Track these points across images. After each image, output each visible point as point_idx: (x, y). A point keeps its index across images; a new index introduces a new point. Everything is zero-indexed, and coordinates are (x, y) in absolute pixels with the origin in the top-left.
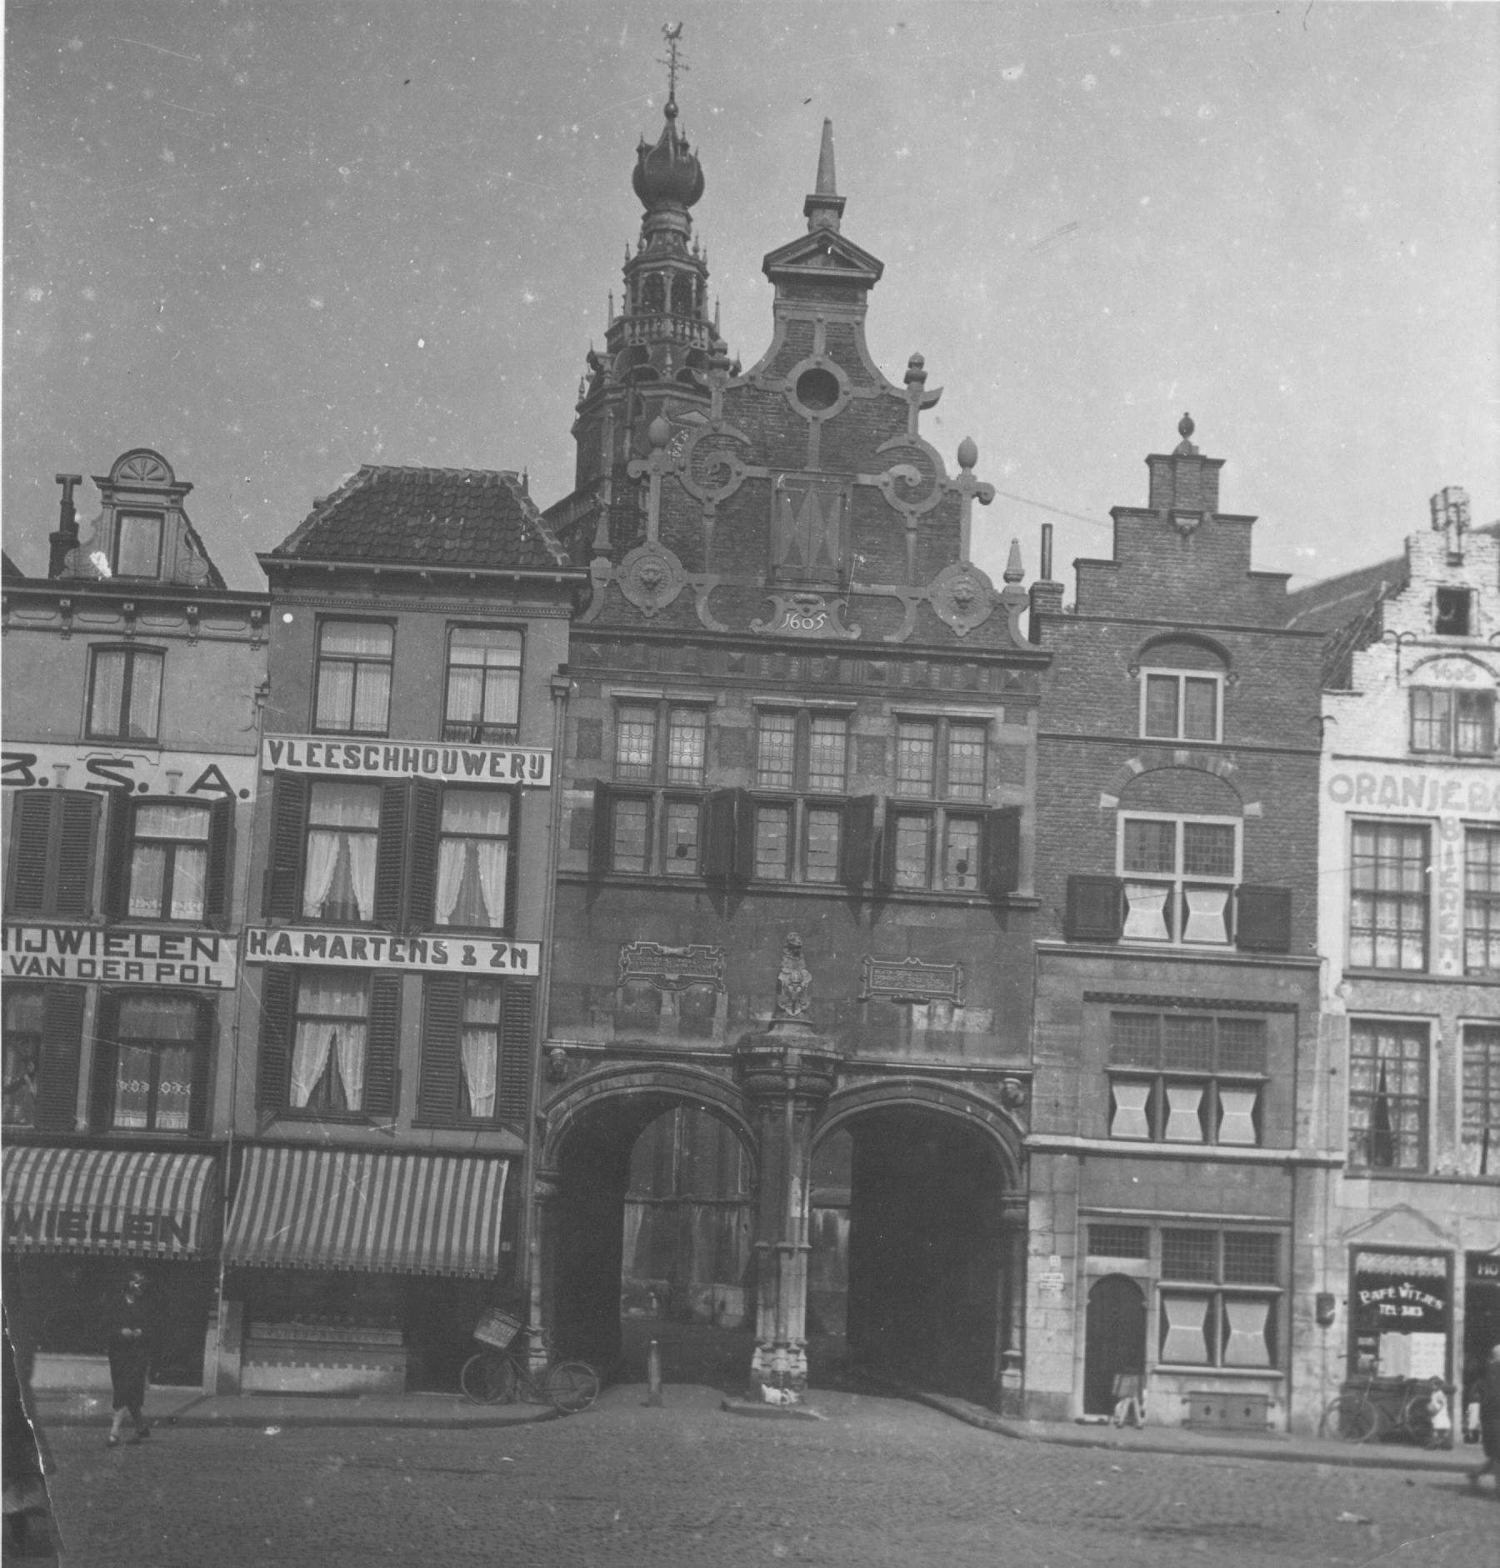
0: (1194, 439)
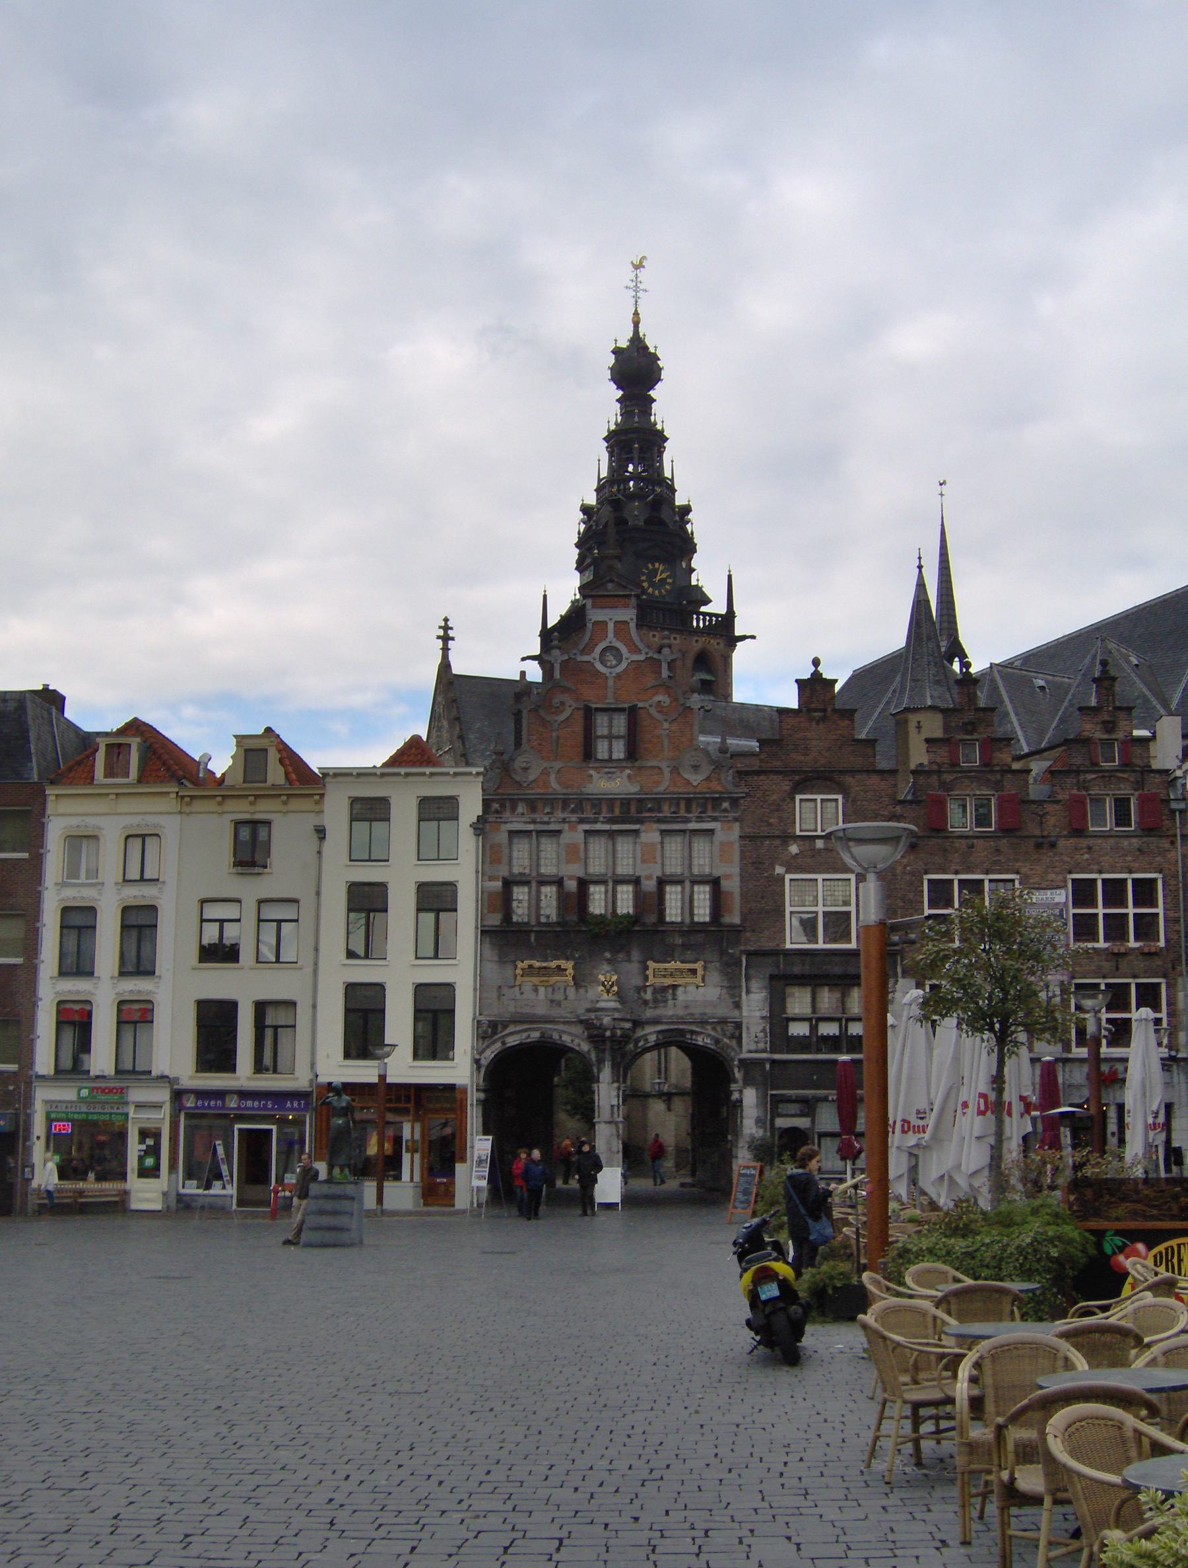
0: (819, 669)
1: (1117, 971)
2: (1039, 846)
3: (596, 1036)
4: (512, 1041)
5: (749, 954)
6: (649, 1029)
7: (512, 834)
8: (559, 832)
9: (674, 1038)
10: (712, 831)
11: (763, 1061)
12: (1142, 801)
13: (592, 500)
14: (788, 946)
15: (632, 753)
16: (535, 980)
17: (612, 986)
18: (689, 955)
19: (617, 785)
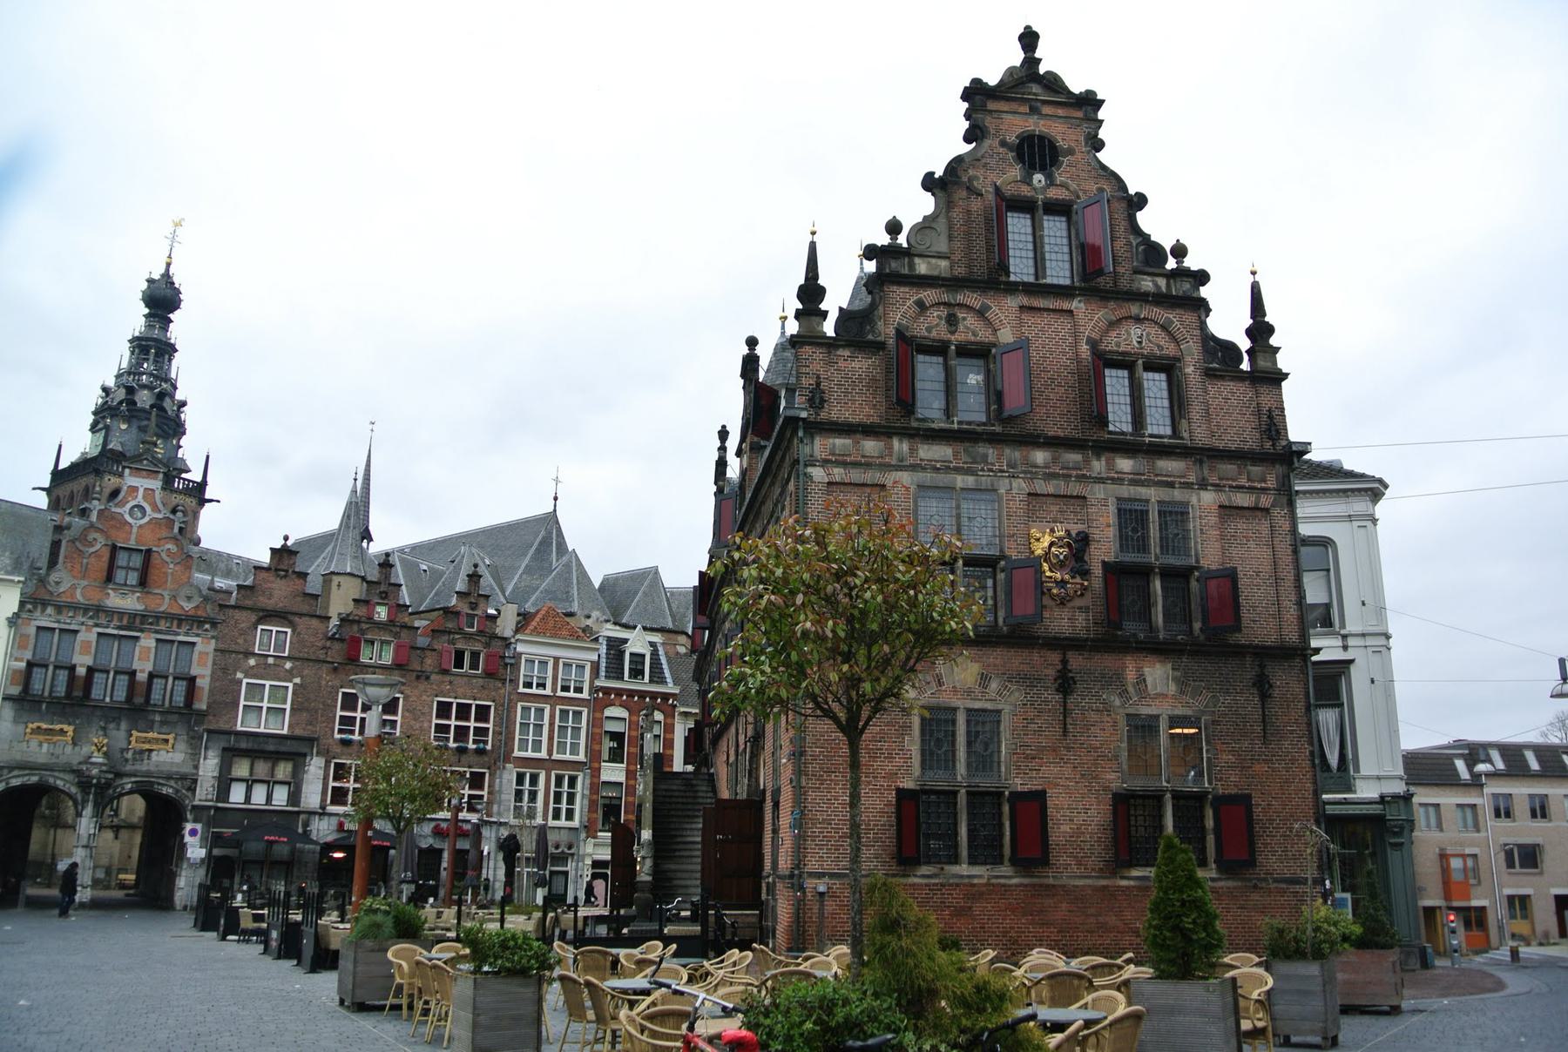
1: (459, 763)
2: (418, 677)
3: (85, 784)
4: (15, 782)
5: (210, 732)
6: (125, 780)
7: (39, 628)
8: (76, 632)
9: (146, 791)
10: (194, 644)
11: (210, 808)
12: (488, 656)
13: (111, 383)
14: (239, 728)
15: (143, 582)
16: (41, 738)
19: (130, 602)
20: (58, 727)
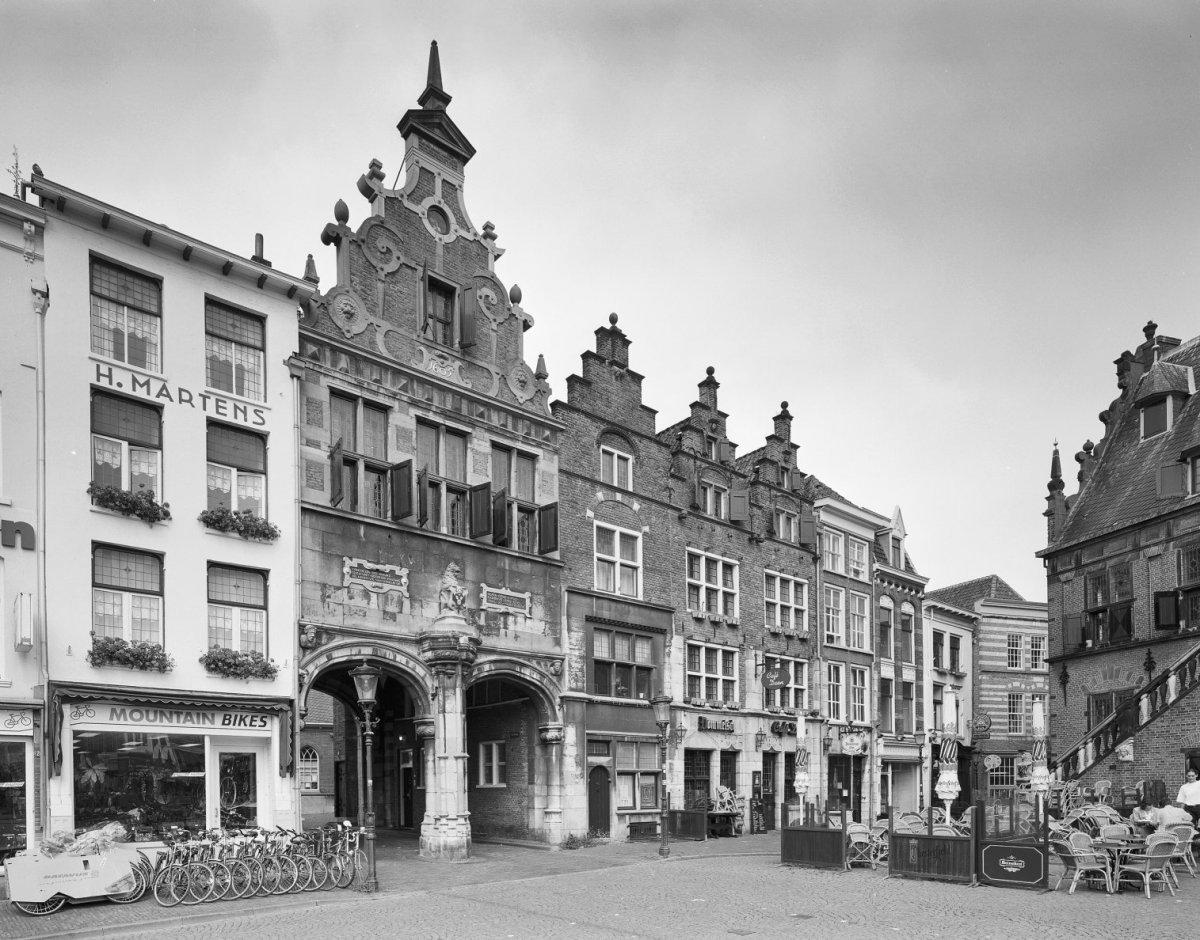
16: (369, 584)
17: (463, 601)
18: (518, 584)
20: (388, 568)
